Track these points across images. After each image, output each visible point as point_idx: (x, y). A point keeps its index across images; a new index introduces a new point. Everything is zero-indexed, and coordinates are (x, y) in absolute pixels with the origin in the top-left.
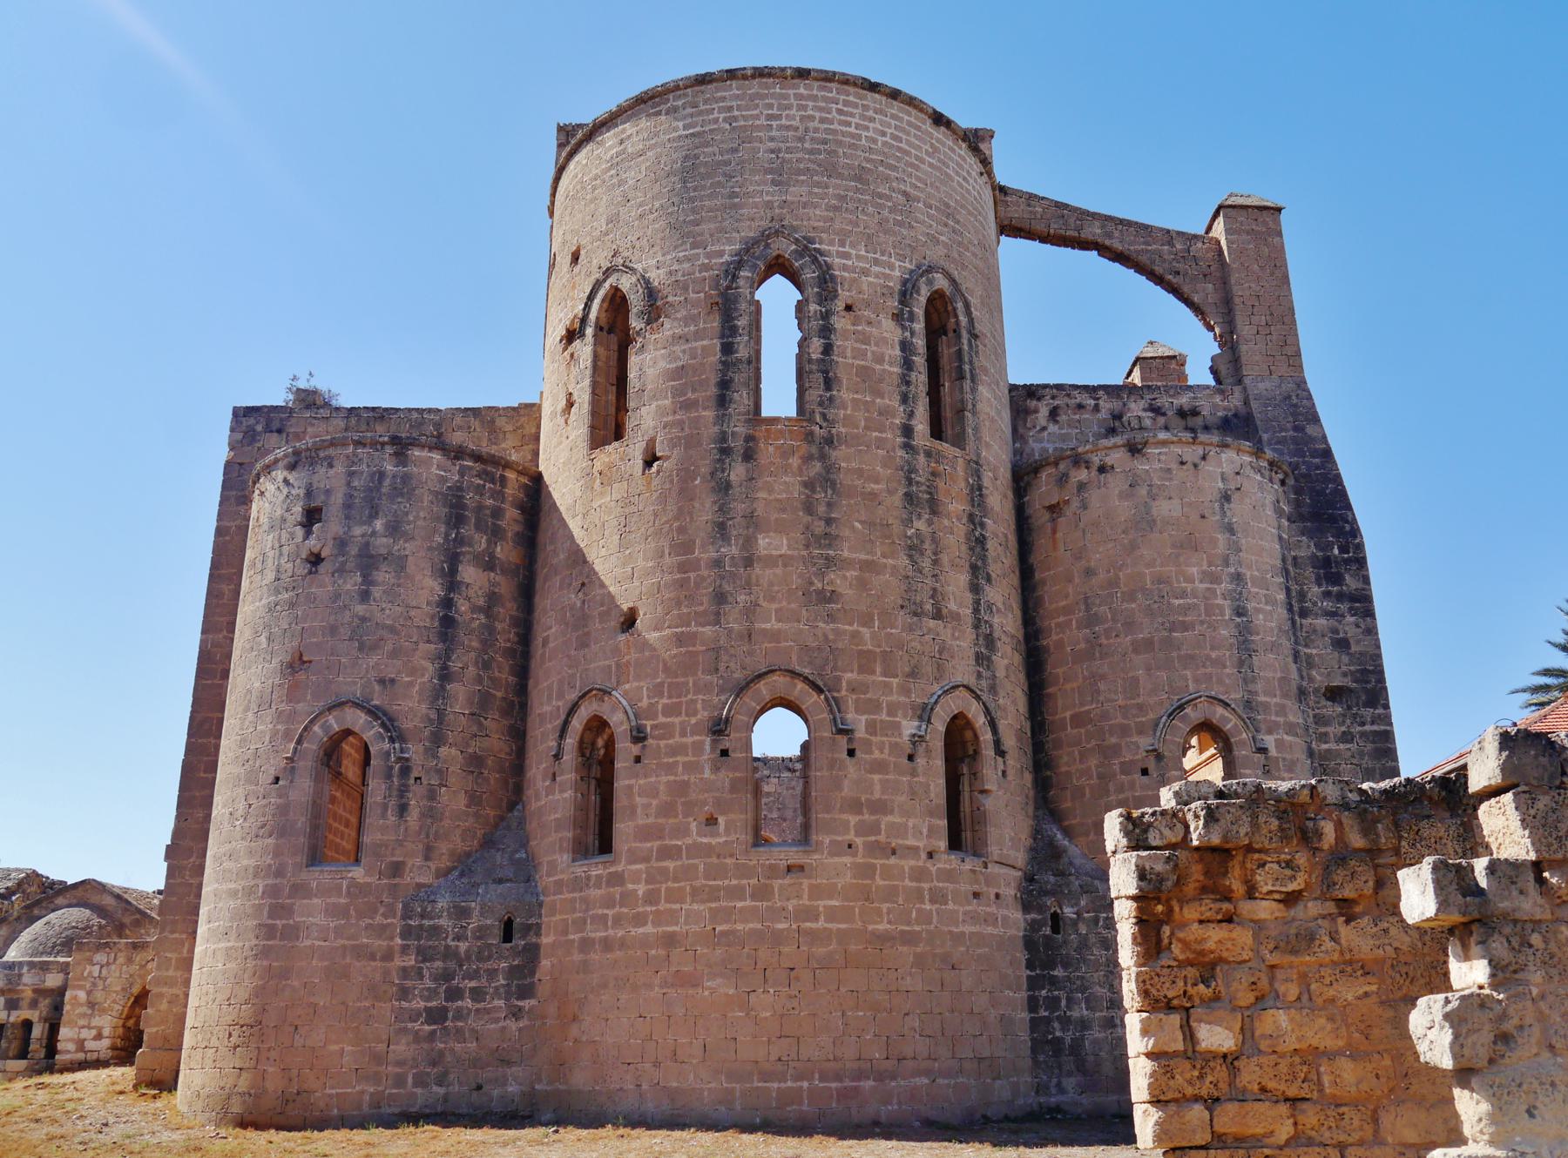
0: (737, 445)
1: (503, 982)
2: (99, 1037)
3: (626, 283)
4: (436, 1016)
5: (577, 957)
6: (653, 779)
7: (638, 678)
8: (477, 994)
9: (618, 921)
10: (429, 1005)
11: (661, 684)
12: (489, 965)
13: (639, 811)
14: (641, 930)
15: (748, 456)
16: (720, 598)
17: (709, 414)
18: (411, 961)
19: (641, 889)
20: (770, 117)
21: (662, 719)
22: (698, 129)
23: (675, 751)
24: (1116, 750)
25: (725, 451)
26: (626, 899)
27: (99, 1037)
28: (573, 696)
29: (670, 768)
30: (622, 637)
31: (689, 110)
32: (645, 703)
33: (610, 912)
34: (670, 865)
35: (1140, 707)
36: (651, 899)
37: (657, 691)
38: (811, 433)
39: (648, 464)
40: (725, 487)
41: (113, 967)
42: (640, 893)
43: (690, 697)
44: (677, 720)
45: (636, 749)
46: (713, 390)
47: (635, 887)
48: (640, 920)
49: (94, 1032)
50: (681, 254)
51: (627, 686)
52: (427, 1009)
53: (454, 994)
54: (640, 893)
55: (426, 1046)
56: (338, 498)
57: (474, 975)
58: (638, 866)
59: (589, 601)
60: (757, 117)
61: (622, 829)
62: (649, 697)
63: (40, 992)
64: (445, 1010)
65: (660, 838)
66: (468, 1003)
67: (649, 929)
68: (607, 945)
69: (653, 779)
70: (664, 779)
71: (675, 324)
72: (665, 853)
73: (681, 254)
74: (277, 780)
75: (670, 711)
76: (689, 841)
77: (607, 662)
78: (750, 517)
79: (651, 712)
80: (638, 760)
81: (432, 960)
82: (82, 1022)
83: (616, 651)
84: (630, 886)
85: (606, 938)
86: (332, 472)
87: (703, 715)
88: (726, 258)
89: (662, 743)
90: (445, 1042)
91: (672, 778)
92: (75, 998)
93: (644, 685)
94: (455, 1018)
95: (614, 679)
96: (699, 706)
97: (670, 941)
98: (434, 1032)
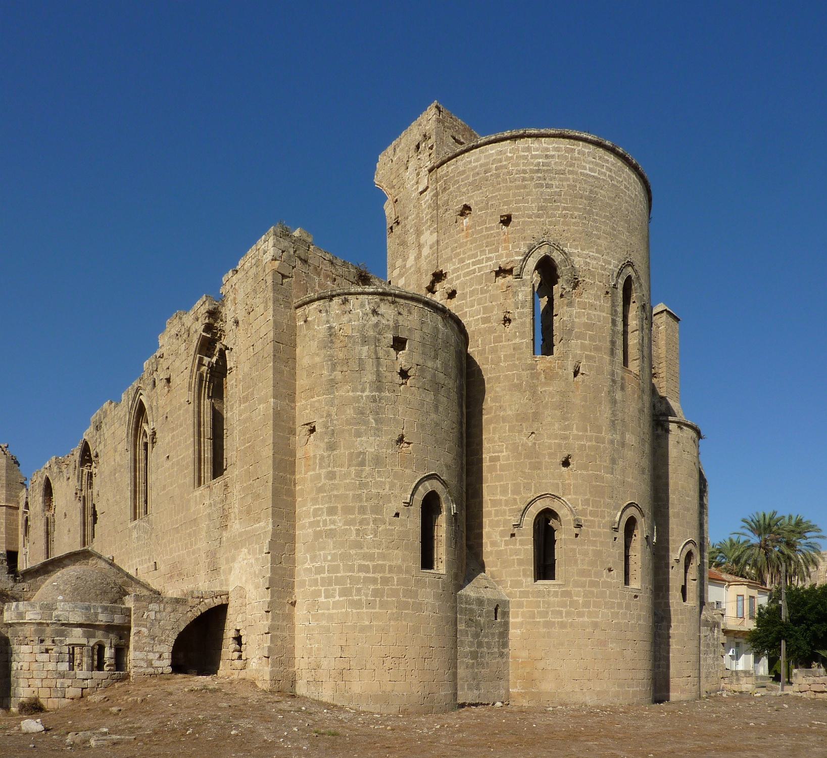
1: (497, 640)
3: (557, 257)
5: (543, 630)
6: (586, 547)
7: (575, 493)
9: (568, 614)
10: (471, 649)
11: (588, 500)
12: (491, 631)
13: (579, 561)
14: (581, 619)
16: (613, 461)
19: (581, 600)
21: (589, 518)
22: (596, 174)
23: (596, 535)
26: (573, 604)
28: (531, 496)
29: (594, 543)
30: (564, 469)
31: (591, 159)
32: (580, 507)
33: (564, 610)
34: (595, 590)
36: (586, 604)
37: (586, 502)
39: (576, 373)
42: (581, 602)
43: (602, 509)
44: (596, 519)
45: (576, 531)
47: (578, 598)
48: (581, 615)
50: (591, 254)
51: (569, 497)
52: (471, 652)
53: (480, 645)
54: (581, 602)
55: (471, 671)
57: (486, 636)
58: (579, 589)
59: (539, 444)
61: (559, 569)
62: (582, 505)
64: (477, 652)
65: (590, 576)
66: (485, 649)
67: (586, 619)
68: (563, 625)
69: (586, 547)
70: (591, 548)
71: (590, 296)
72: (594, 584)
73: (591, 254)
75: (592, 514)
76: (602, 579)
77: (556, 481)
80: (577, 535)
81: (470, 627)
84: (575, 598)
85: (562, 622)
87: (607, 519)
89: (590, 530)
90: (478, 669)
91: (595, 548)
93: (580, 498)
94: (481, 657)
95: (561, 491)
96: (606, 515)
97: (595, 625)
98: (474, 663)
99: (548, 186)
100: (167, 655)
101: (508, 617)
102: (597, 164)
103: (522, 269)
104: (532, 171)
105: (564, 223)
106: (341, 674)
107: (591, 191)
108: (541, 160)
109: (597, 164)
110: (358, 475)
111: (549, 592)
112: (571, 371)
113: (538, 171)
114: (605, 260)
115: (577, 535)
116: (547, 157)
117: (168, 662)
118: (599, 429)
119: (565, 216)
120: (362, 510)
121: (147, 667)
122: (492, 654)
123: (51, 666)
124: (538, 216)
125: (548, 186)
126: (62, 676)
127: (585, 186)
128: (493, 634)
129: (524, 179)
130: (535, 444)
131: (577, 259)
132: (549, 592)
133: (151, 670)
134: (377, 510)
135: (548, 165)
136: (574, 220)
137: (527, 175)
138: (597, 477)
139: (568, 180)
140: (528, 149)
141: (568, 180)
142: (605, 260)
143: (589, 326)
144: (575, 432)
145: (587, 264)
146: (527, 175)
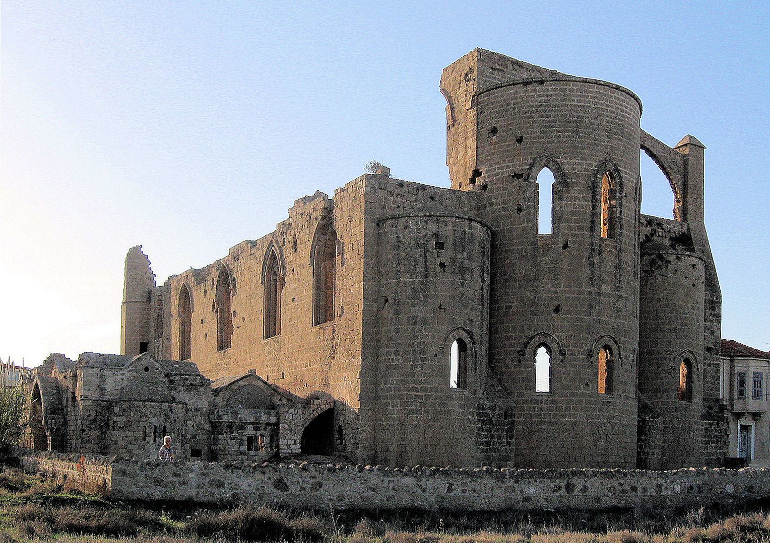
0: (597, 248)
2: (295, 443)
4: (487, 444)
8: (499, 437)
15: (600, 253)
16: (591, 307)
17: (587, 233)
18: (480, 425)
20: (607, 106)
23: (574, 360)
24: (662, 365)
25: (593, 250)
26: (559, 409)
27: (295, 443)
29: (574, 366)
35: (670, 351)
38: (616, 247)
40: (592, 264)
41: (297, 415)
45: (562, 357)
46: (589, 225)
48: (564, 416)
49: (293, 441)
52: (485, 441)
53: (492, 437)
56: (450, 241)
60: (602, 104)
63: (268, 424)
68: (550, 423)
71: (575, 191)
72: (573, 395)
74: (436, 355)
78: (600, 277)
79: (567, 345)
82: (287, 437)
83: (552, 320)
84: (560, 405)
86: (447, 228)
88: (593, 168)
92: (284, 427)
94: (493, 445)
97: (574, 423)
98: (487, 449)
99: (548, 116)
100: (298, 442)
101: (515, 417)
102: (584, 96)
103: (529, 175)
104: (537, 106)
105: (559, 142)
106: (401, 454)
107: (578, 117)
108: (543, 98)
109: (584, 96)
110: (413, 330)
111: (542, 400)
112: (561, 245)
113: (540, 106)
114: (587, 165)
115: (562, 361)
116: (547, 96)
117: (299, 446)
118: (580, 285)
119: (559, 137)
120: (414, 352)
121: (288, 449)
122: (501, 443)
123: (236, 448)
124: (541, 138)
125: (548, 116)
126: (242, 453)
127: (574, 114)
128: (503, 430)
129: (531, 112)
130: (535, 297)
131: (566, 166)
132: (542, 400)
133: (289, 451)
134: (423, 352)
135: (548, 101)
136: (564, 139)
137: (534, 109)
138: (577, 320)
139: (561, 111)
140: (535, 91)
141: (561, 111)
142: (587, 165)
143: (573, 213)
144: (563, 288)
145: (574, 169)
146: (534, 109)
